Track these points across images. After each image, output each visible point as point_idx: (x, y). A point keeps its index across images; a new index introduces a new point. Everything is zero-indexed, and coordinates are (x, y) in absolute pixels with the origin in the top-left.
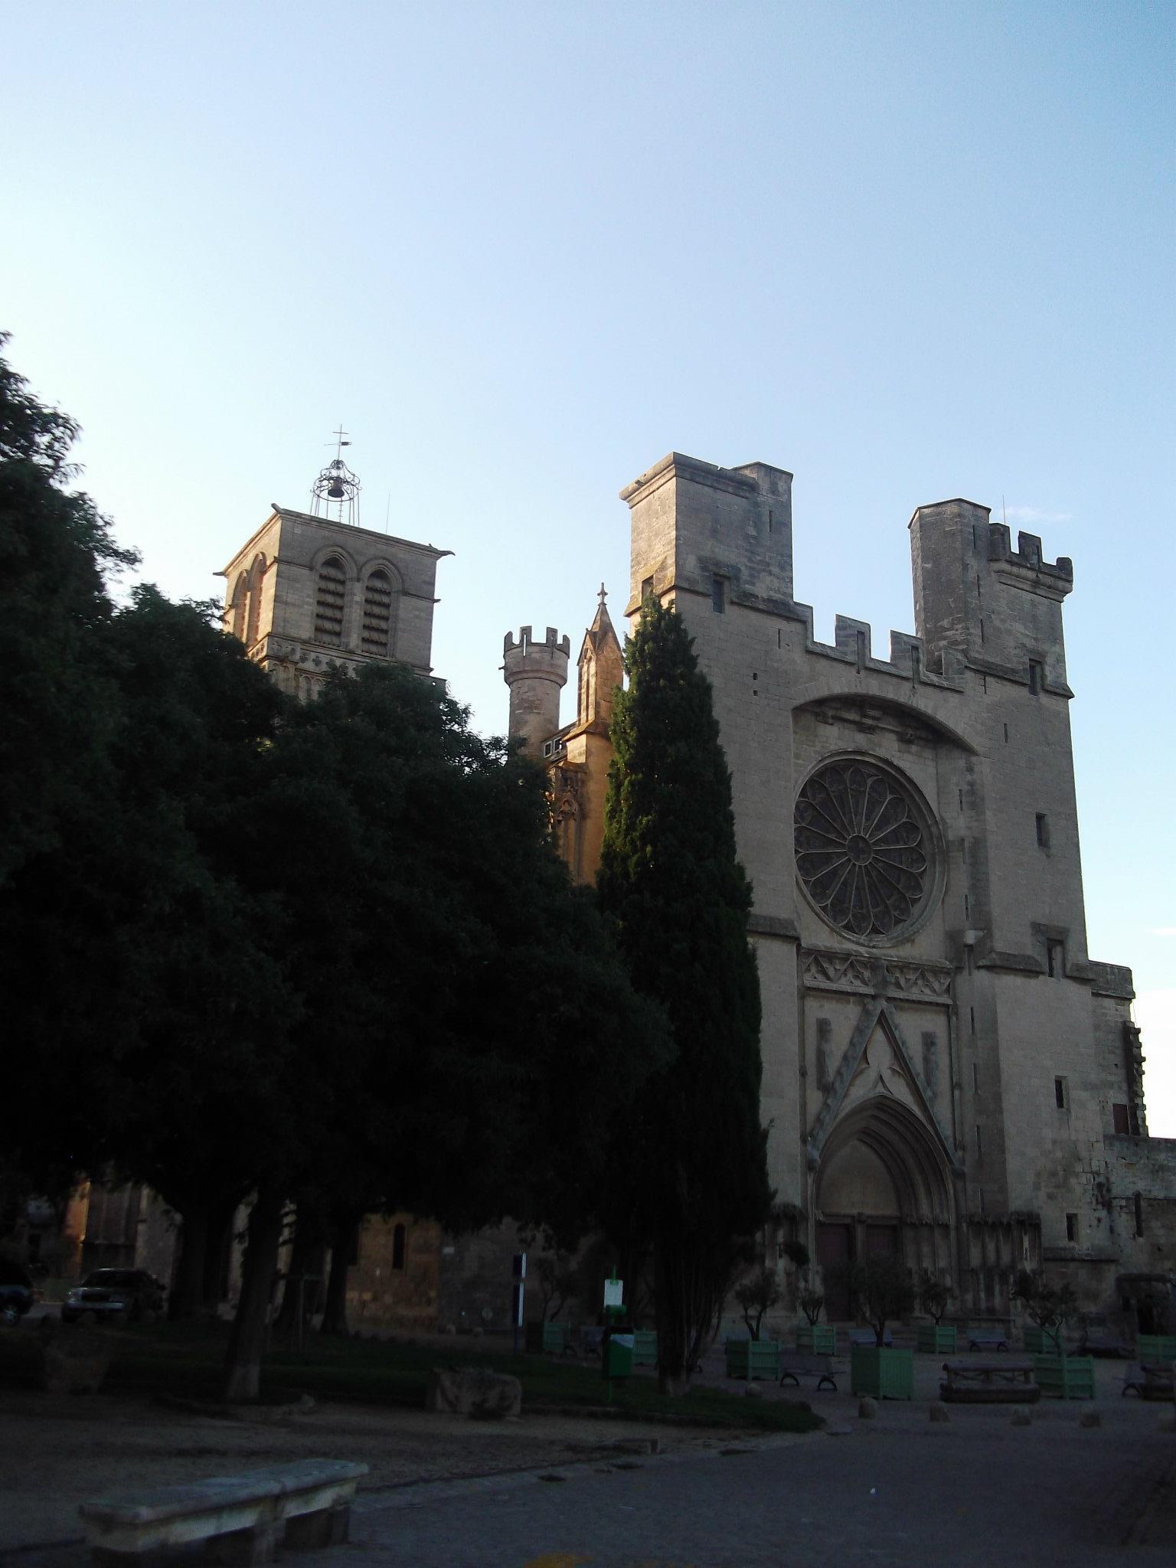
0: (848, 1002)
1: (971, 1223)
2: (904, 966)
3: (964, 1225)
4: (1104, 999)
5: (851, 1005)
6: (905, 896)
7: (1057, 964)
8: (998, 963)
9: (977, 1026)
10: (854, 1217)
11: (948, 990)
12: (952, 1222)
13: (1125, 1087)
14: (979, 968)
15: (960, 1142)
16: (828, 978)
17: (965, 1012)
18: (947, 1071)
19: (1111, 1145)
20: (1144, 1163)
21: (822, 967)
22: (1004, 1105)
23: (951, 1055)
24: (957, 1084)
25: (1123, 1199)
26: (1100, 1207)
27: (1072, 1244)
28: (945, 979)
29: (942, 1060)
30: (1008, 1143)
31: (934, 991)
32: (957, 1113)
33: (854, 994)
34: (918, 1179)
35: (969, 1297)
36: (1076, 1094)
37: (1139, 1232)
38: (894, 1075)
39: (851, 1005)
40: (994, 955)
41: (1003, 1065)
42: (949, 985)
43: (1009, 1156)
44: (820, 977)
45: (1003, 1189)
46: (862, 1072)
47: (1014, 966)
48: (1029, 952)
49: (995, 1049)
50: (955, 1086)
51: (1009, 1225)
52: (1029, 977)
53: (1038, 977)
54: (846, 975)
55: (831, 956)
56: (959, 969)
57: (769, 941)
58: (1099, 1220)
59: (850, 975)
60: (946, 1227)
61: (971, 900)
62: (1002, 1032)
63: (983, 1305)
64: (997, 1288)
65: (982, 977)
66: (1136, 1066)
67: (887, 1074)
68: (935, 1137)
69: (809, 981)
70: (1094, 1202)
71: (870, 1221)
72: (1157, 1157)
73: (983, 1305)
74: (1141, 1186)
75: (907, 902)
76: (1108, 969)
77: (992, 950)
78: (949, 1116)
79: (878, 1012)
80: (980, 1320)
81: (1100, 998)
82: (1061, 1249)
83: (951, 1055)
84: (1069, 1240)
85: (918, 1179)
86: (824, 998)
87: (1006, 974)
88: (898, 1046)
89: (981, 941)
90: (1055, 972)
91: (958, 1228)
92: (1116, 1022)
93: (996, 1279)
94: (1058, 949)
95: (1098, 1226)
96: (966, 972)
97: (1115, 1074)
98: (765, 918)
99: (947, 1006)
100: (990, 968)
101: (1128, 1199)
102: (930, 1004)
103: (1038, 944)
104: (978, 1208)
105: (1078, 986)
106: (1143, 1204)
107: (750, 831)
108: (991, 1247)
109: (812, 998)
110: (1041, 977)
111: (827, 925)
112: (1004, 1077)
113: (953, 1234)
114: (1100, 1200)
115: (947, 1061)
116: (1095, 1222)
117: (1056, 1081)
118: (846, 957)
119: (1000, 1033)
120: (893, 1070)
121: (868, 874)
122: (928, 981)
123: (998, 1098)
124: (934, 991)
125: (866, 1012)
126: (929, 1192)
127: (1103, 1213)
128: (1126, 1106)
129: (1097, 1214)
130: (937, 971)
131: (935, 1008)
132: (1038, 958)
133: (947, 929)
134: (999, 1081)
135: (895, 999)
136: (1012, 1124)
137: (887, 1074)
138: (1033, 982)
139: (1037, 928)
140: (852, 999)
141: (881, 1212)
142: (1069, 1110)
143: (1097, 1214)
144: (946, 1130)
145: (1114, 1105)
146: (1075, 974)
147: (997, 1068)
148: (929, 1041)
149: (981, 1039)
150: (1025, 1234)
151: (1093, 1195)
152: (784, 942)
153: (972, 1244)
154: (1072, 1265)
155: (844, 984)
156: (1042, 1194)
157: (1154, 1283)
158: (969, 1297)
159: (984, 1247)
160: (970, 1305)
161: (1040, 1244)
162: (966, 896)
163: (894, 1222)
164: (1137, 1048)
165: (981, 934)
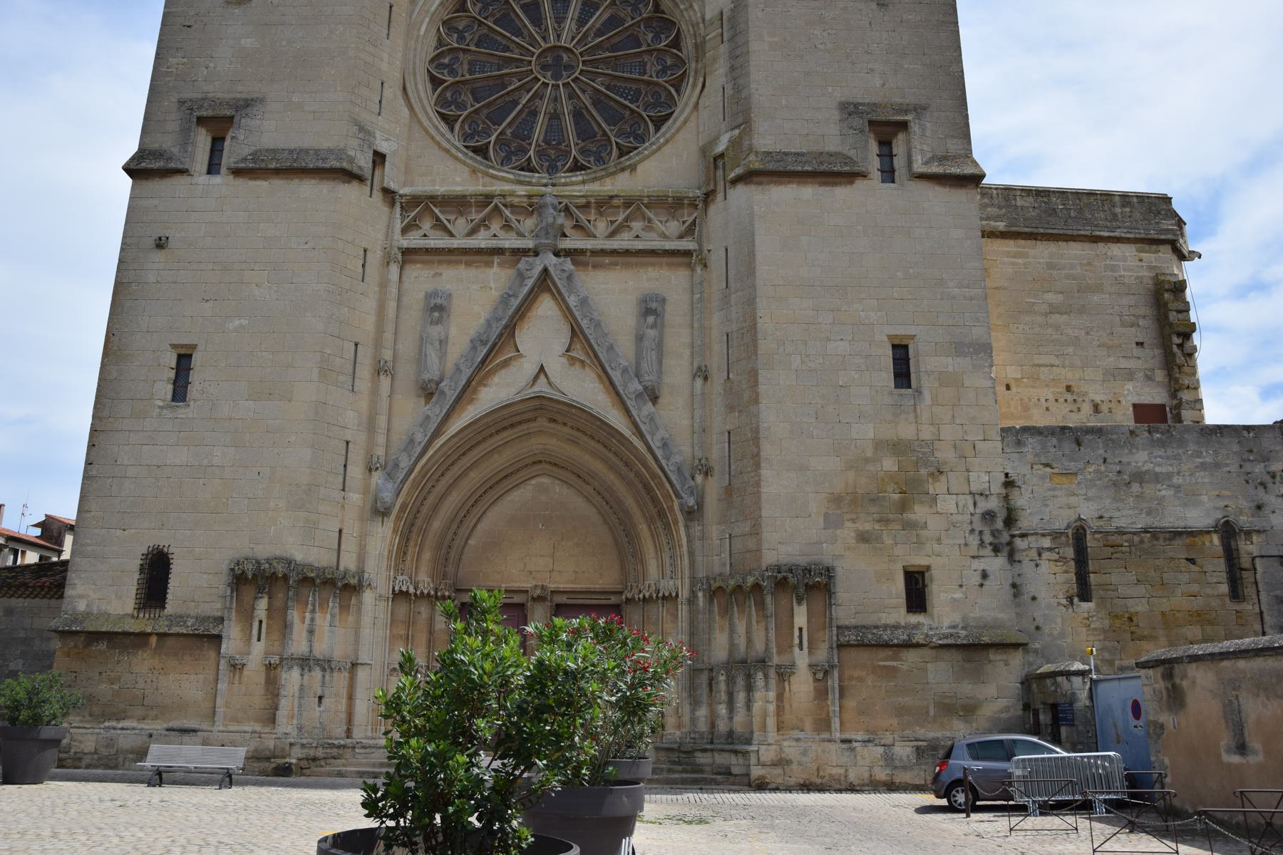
0: (489, 264)
1: (713, 593)
2: (604, 204)
3: (700, 594)
4: (1110, 245)
5: (495, 269)
6: (642, 117)
7: (899, 163)
8: (757, 166)
9: (732, 273)
10: (527, 591)
11: (690, 231)
12: (684, 594)
13: (1160, 375)
14: (735, 182)
15: (700, 461)
16: (451, 235)
17: (716, 260)
18: (687, 352)
19: (1019, 443)
20: (1098, 471)
21: (438, 219)
22: (762, 388)
23: (692, 327)
24: (699, 368)
25: (1043, 535)
26: (988, 551)
27: (914, 619)
28: (690, 215)
29: (678, 339)
30: (767, 449)
31: (665, 237)
32: (698, 413)
33: (499, 251)
34: (643, 528)
35: (702, 712)
36: (925, 363)
37: (1084, 592)
38: (572, 365)
39: (495, 269)
40: (752, 157)
41: (764, 324)
42: (695, 220)
43: (765, 472)
44: (439, 233)
45: (756, 531)
46: (506, 364)
47: (791, 168)
48: (833, 145)
49: (751, 302)
50: (703, 374)
51: (757, 587)
52: (834, 184)
53: (852, 183)
54: (487, 227)
55: (458, 203)
56: (708, 197)
57: (296, 181)
58: (985, 575)
59: (496, 226)
60: (670, 599)
61: (729, 92)
62: (762, 271)
63: (722, 727)
64: (741, 697)
65: (740, 194)
66: (1176, 340)
67: (556, 366)
68: (649, 457)
69: (414, 241)
70: (974, 541)
71: (563, 599)
72: (1125, 460)
73: (722, 727)
74: (1087, 511)
75: (646, 122)
76: (1117, 199)
77: (751, 150)
78: (686, 422)
79: (539, 269)
80: (712, 750)
81: (1101, 245)
82: (886, 627)
83: (692, 327)
84: (908, 612)
85: (643, 528)
86: (440, 262)
87: (780, 183)
88: (575, 319)
89: (735, 144)
90: (897, 174)
91: (692, 601)
92: (1140, 278)
93: (740, 682)
94: (901, 137)
95: (981, 585)
96: (720, 196)
97: (1139, 358)
98: (291, 151)
99: (688, 253)
100: (749, 177)
101: (1056, 535)
102: (653, 253)
103: (851, 131)
104: (724, 565)
105: (947, 190)
106: (1090, 542)
107: (284, 43)
108: (741, 628)
109: (419, 266)
110: (860, 183)
111: (464, 163)
112: (763, 346)
113: (683, 611)
114: (988, 538)
115: (687, 339)
116: (977, 579)
117: (894, 347)
118: (486, 200)
119: (758, 274)
120: (573, 360)
121: (572, 96)
122: (650, 221)
123: (753, 375)
124: (665, 237)
125: (521, 276)
126: (658, 550)
127: (996, 564)
128: (1163, 407)
129: (979, 565)
130: (672, 204)
131: (665, 260)
132: (852, 153)
133: (701, 144)
134: (755, 352)
135: (582, 252)
136: (771, 417)
137: (556, 366)
138: (841, 193)
139: (849, 109)
140: (496, 260)
141: (578, 586)
142: (919, 391)
143: (979, 565)
144: (684, 450)
145: (1135, 406)
146: (935, 169)
147: (753, 328)
148: (651, 309)
149: (736, 292)
150: (799, 603)
151: (972, 531)
152: (322, 179)
153: (717, 625)
154: (911, 656)
155: (482, 240)
156: (847, 533)
157: (1059, 679)
158: (702, 712)
159: (732, 631)
160: (703, 727)
161: (831, 619)
162: (724, 88)
163: (614, 600)
164: (1179, 312)
165: (737, 132)
